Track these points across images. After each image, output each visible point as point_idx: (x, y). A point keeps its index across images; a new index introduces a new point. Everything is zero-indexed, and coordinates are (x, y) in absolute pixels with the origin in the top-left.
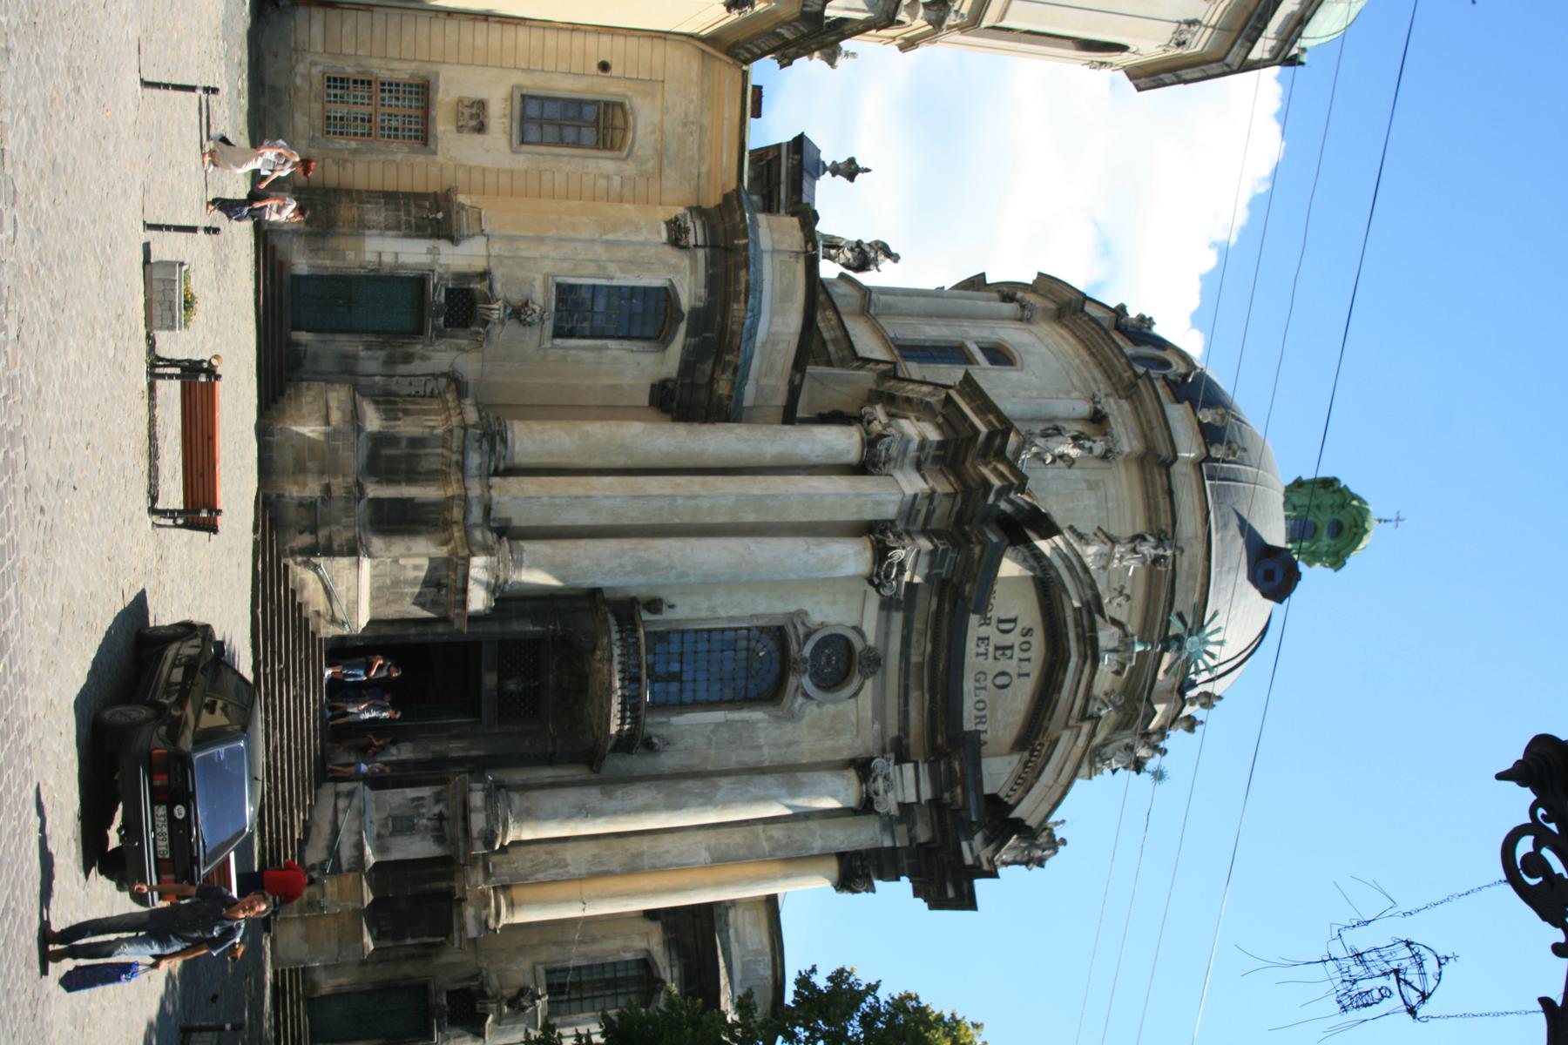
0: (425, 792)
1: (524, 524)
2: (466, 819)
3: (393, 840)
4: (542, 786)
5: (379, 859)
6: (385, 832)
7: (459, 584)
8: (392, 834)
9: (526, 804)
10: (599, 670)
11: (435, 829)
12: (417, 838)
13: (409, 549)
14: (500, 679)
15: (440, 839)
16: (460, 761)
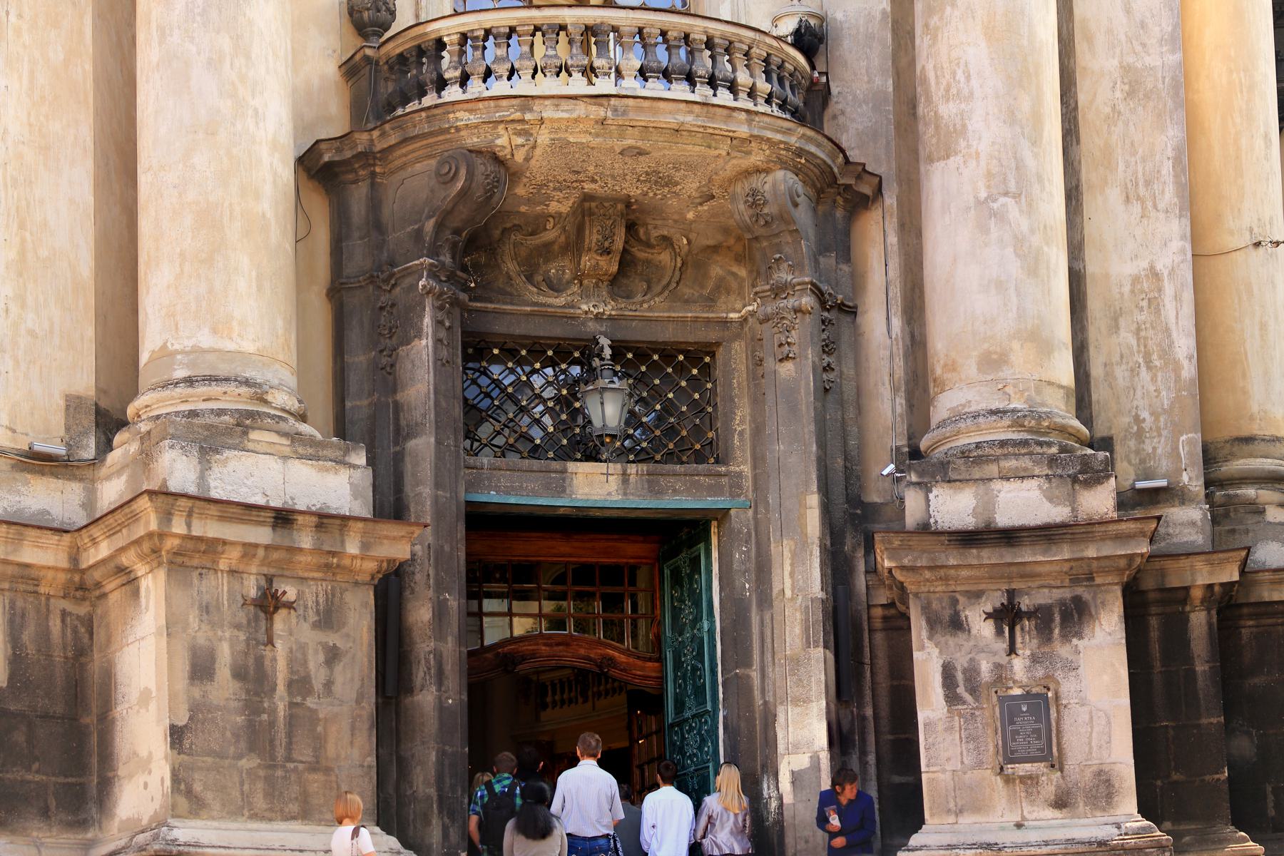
0: (928, 662)
1: (90, 362)
2: (1010, 536)
3: (1075, 757)
4: (916, 344)
5: (1128, 805)
6: (1050, 783)
7: (262, 535)
8: (1057, 764)
9: (970, 369)
10: (560, 146)
11: (1044, 631)
12: (1068, 687)
13: (145, 696)
14: (591, 456)
15: (1074, 616)
16: (837, 569)
